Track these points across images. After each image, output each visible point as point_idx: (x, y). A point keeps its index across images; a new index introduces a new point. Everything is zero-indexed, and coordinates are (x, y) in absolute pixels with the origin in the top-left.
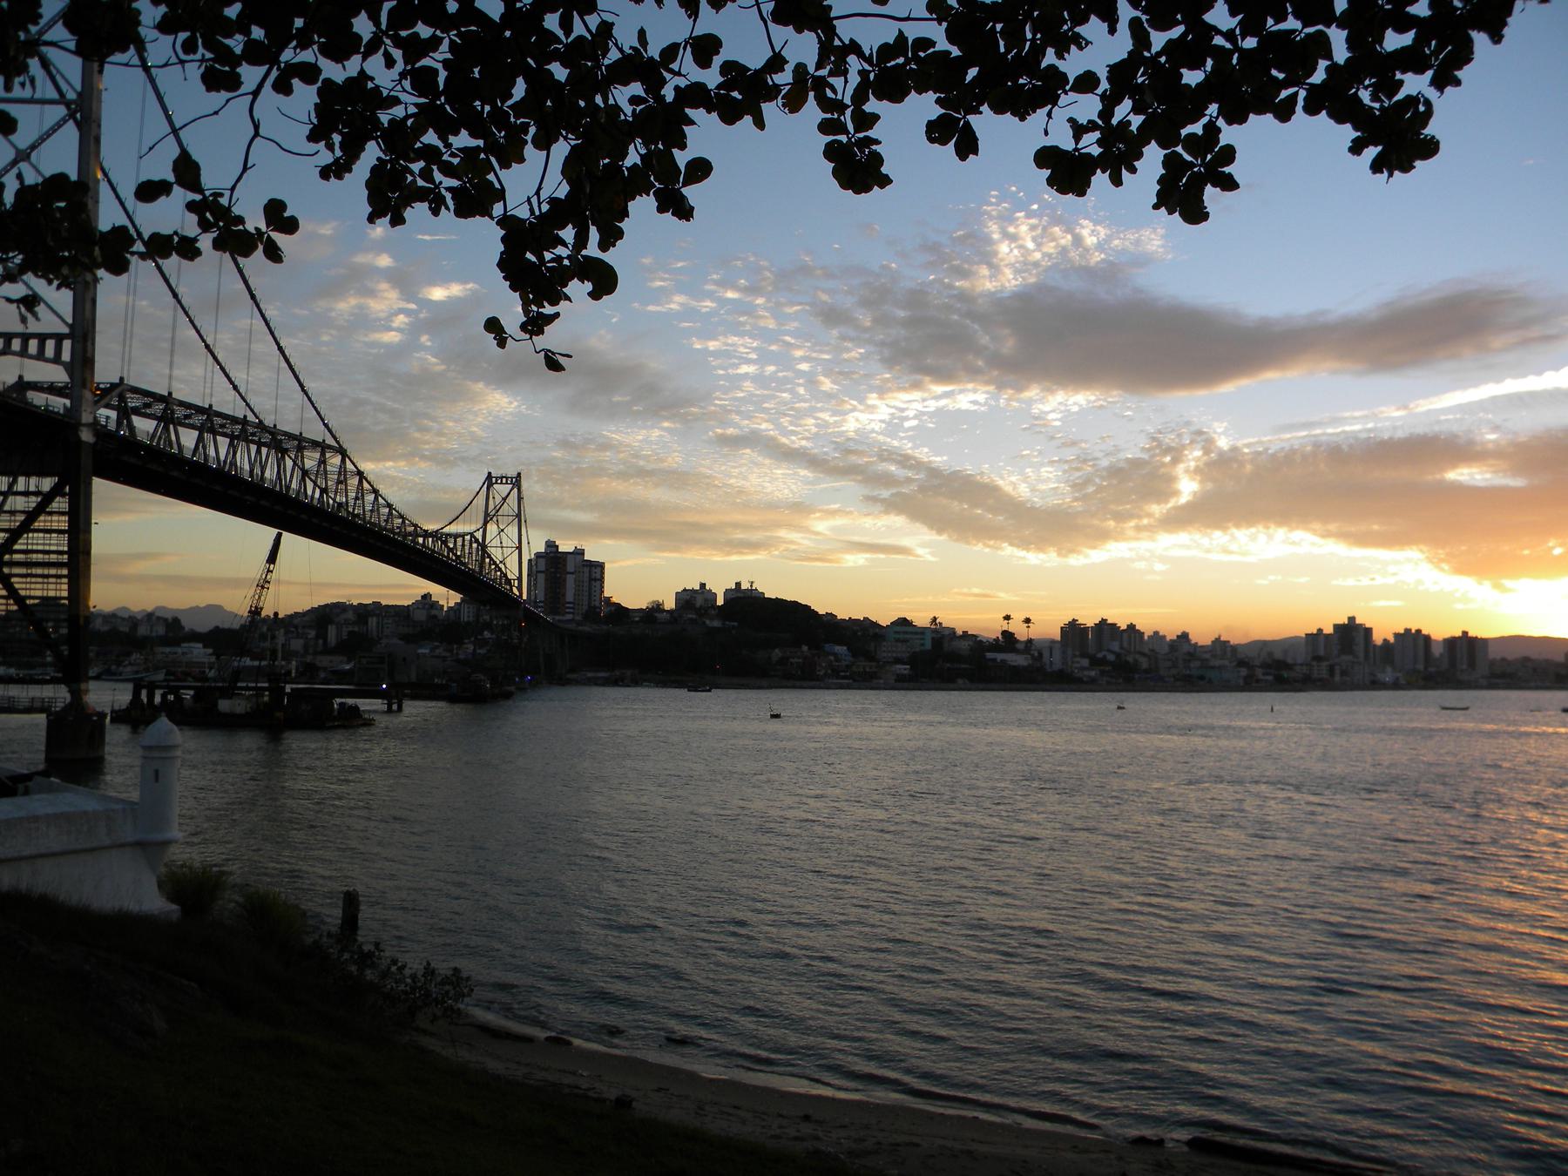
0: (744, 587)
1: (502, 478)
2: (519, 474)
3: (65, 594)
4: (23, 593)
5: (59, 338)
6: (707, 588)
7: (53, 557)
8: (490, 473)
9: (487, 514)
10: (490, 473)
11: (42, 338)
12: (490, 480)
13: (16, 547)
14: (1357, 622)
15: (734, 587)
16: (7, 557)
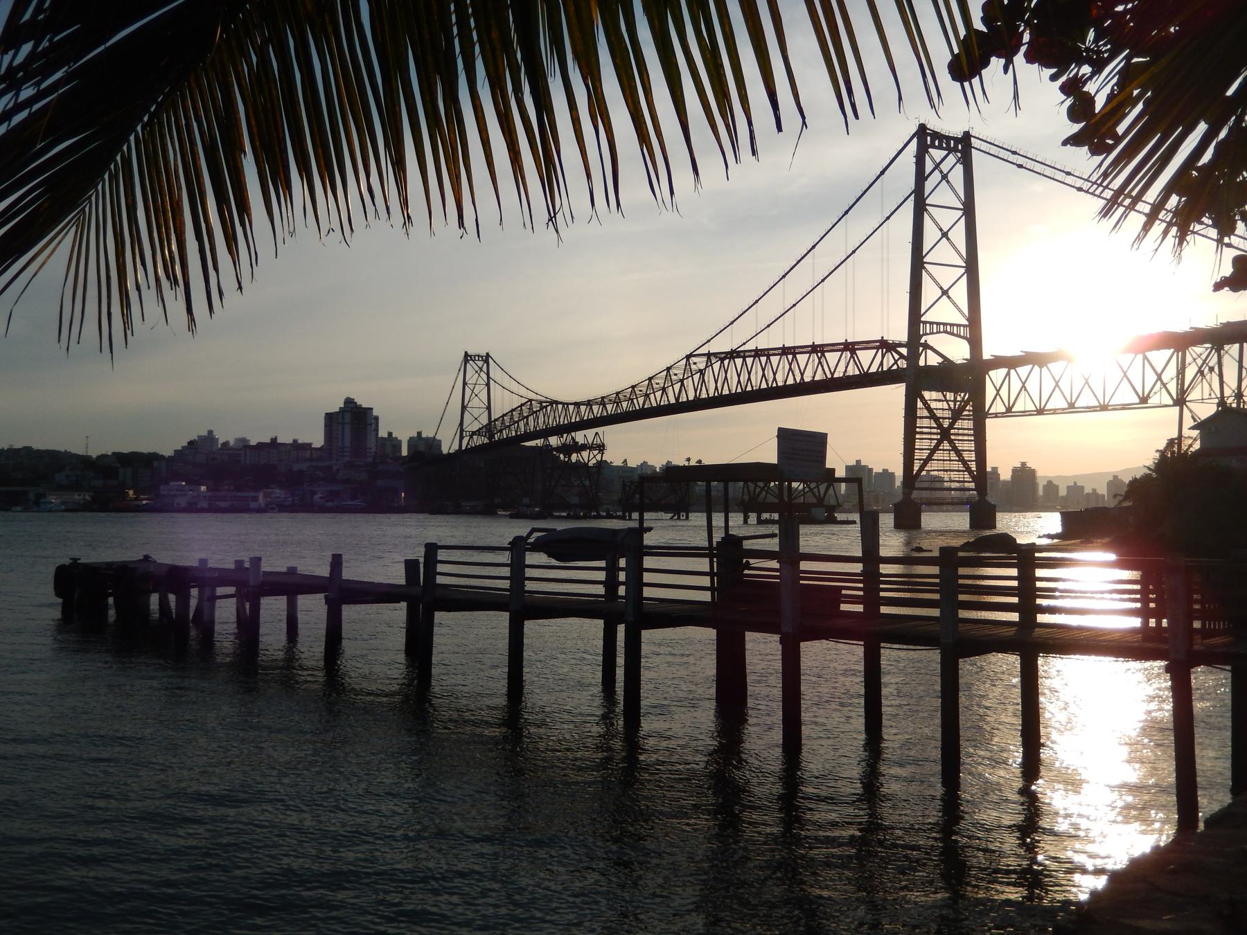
0: (424, 435)
1: (475, 356)
2: (488, 354)
3: (973, 449)
4: (960, 448)
5: (964, 326)
6: (394, 436)
7: (966, 432)
8: (466, 352)
9: (465, 384)
10: (466, 352)
11: (958, 326)
12: (467, 358)
13: (956, 426)
14: (862, 464)
15: (416, 435)
16: (952, 431)
